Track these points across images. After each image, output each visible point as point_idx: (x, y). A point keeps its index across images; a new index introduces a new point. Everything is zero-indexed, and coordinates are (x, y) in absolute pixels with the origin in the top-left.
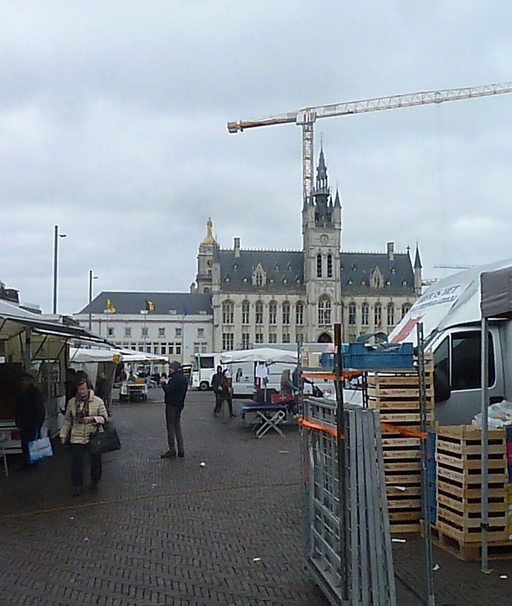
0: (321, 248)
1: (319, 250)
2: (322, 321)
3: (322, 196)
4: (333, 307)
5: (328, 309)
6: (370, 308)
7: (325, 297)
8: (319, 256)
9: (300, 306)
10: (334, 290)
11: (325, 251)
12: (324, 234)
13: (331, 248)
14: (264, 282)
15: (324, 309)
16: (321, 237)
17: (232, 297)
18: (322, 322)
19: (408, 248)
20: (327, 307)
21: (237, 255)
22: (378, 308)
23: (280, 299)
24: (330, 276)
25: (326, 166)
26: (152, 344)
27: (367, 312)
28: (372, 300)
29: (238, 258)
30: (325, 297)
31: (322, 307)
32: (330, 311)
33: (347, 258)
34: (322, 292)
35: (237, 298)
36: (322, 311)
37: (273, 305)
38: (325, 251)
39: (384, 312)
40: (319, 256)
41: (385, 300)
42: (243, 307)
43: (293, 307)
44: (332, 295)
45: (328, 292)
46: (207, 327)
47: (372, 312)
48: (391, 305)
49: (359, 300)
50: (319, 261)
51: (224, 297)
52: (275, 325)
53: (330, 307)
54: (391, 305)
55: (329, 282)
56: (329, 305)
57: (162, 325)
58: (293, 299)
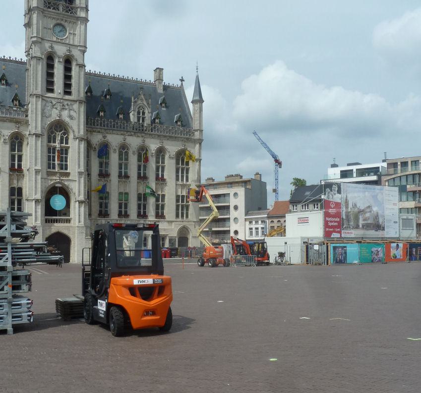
2: (54, 164)
8: (50, 59)
10: (76, 119)
11: (61, 51)
12: (58, 22)
15: (57, 145)
16: (55, 26)
18: (54, 168)
19: (182, 80)
20: (62, 142)
24: (67, 92)
27: (127, 159)
28: (134, 142)
31: (55, 142)
34: (54, 115)
38: (61, 51)
40: (50, 59)
47: (133, 160)
48: (161, 152)
49: (114, 140)
50: (50, 67)
53: (67, 143)
54: (161, 152)
55: (66, 103)
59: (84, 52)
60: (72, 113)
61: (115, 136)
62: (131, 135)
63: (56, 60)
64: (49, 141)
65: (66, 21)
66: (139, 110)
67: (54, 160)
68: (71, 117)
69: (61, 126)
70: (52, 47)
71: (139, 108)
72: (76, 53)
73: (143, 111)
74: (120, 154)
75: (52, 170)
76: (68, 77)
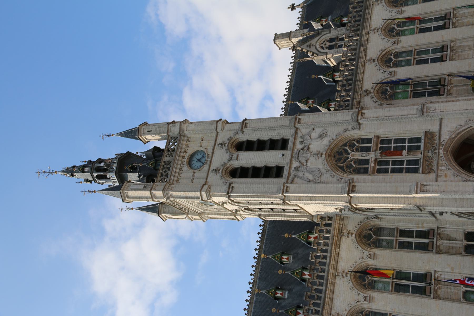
2: (409, 162)
9: (372, 236)
11: (220, 158)
12: (185, 161)
15: (372, 156)
27: (409, 53)
28: (376, 44)
31: (367, 162)
38: (220, 158)
44: (334, 133)
45: (319, 145)
47: (409, 42)
55: (299, 146)
56: (363, 144)
58: (350, 255)
59: (227, 123)
61: (366, 75)
62: (365, 51)
64: (366, 171)
65: (185, 152)
66: (327, 48)
67: (401, 162)
68: (321, 136)
69: (339, 153)
70: (216, 171)
71: (323, 49)
72: (224, 137)
73: (328, 41)
74: (398, 64)
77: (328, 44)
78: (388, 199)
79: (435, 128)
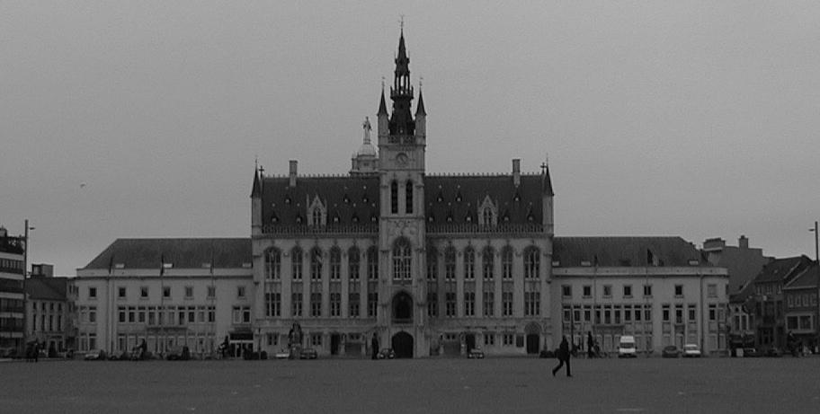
0: (397, 173)
1: (394, 175)
3: (402, 98)
4: (414, 253)
5: (407, 257)
6: (476, 256)
7: (402, 243)
8: (394, 184)
9: (373, 253)
10: (416, 233)
11: (402, 177)
13: (411, 172)
14: (324, 221)
16: (397, 157)
17: (279, 243)
21: (293, 183)
22: (488, 254)
23: (345, 245)
25: (407, 56)
26: (127, 309)
28: (479, 245)
29: (293, 188)
30: (402, 243)
31: (399, 255)
32: (410, 261)
33: (431, 182)
34: (397, 233)
35: (285, 245)
36: (399, 260)
37: (335, 253)
39: (498, 262)
41: (498, 244)
42: (294, 258)
43: (364, 256)
44: (412, 238)
45: (407, 233)
46: (247, 284)
50: (395, 191)
51: (267, 244)
52: (300, 280)
54: (507, 252)
57: (189, 283)
60: (414, 229)
63: (399, 185)
68: (411, 233)
70: (394, 175)
74: (466, 256)
75: (397, 279)
76: (409, 198)
77: (487, 212)
78: (386, 266)
79: (414, 284)
